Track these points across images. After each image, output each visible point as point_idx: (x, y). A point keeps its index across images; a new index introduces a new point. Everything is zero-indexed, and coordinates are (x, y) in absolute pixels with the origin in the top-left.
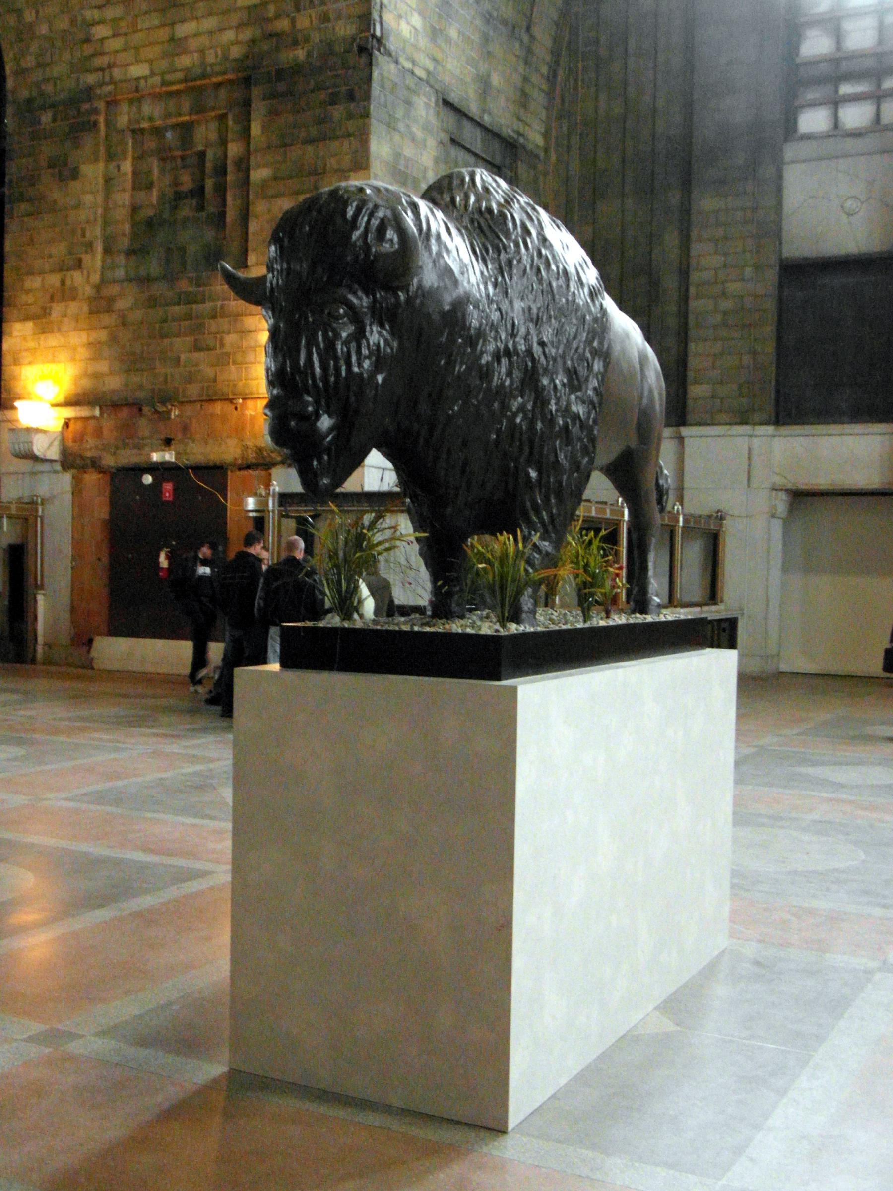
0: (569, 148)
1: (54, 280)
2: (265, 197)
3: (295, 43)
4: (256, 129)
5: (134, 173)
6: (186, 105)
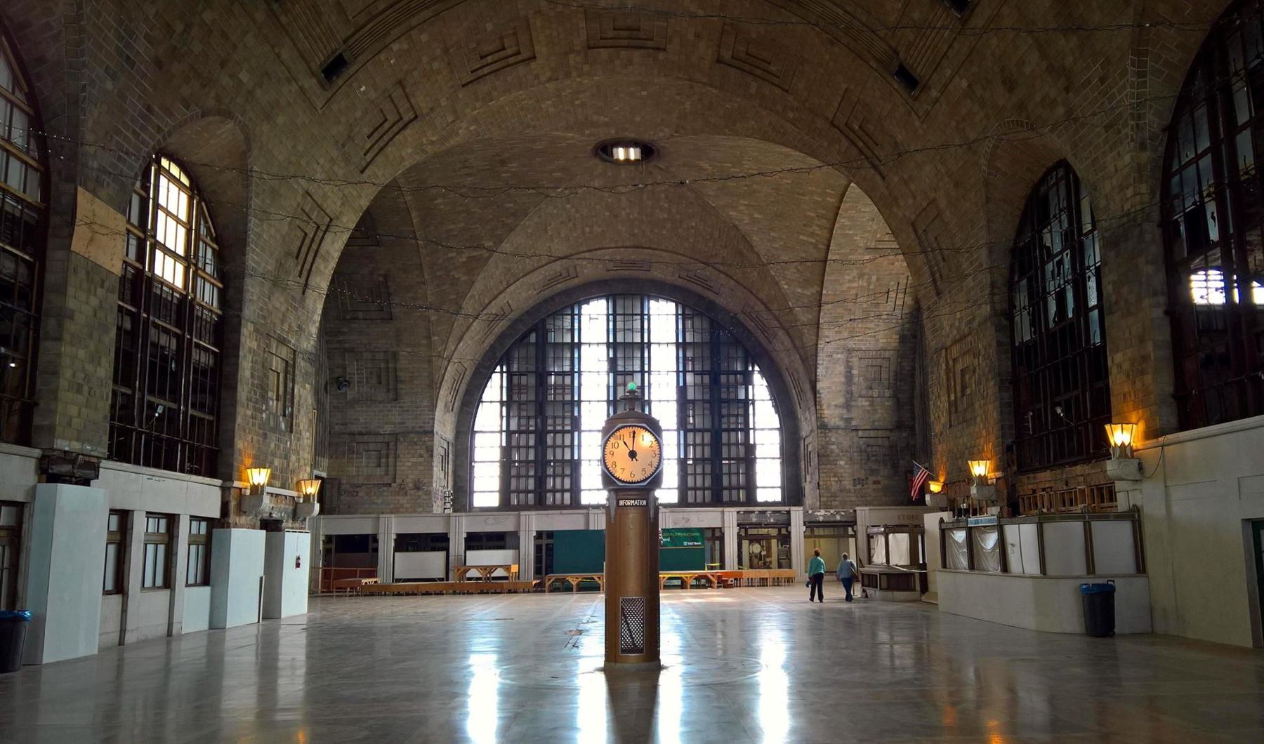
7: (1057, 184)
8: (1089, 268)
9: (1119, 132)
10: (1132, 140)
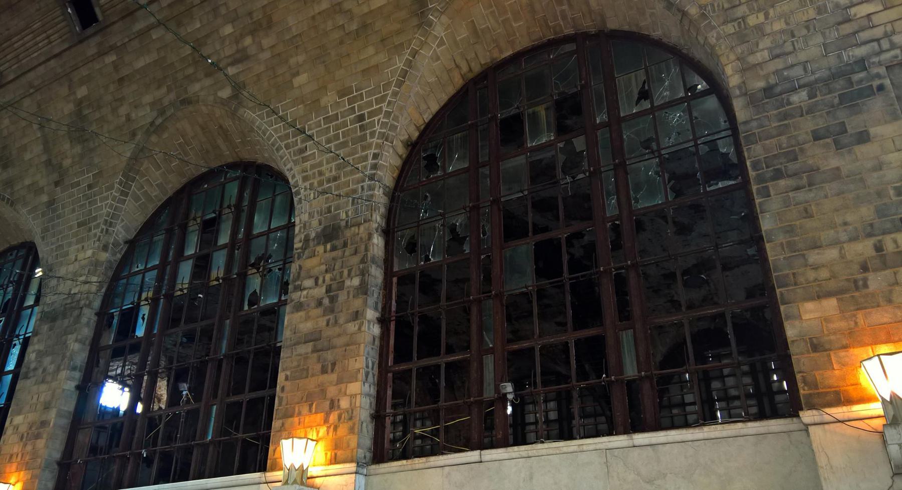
1: (864, 248)
7: (14, 261)
8: (18, 336)
9: (90, 230)
10: (99, 240)
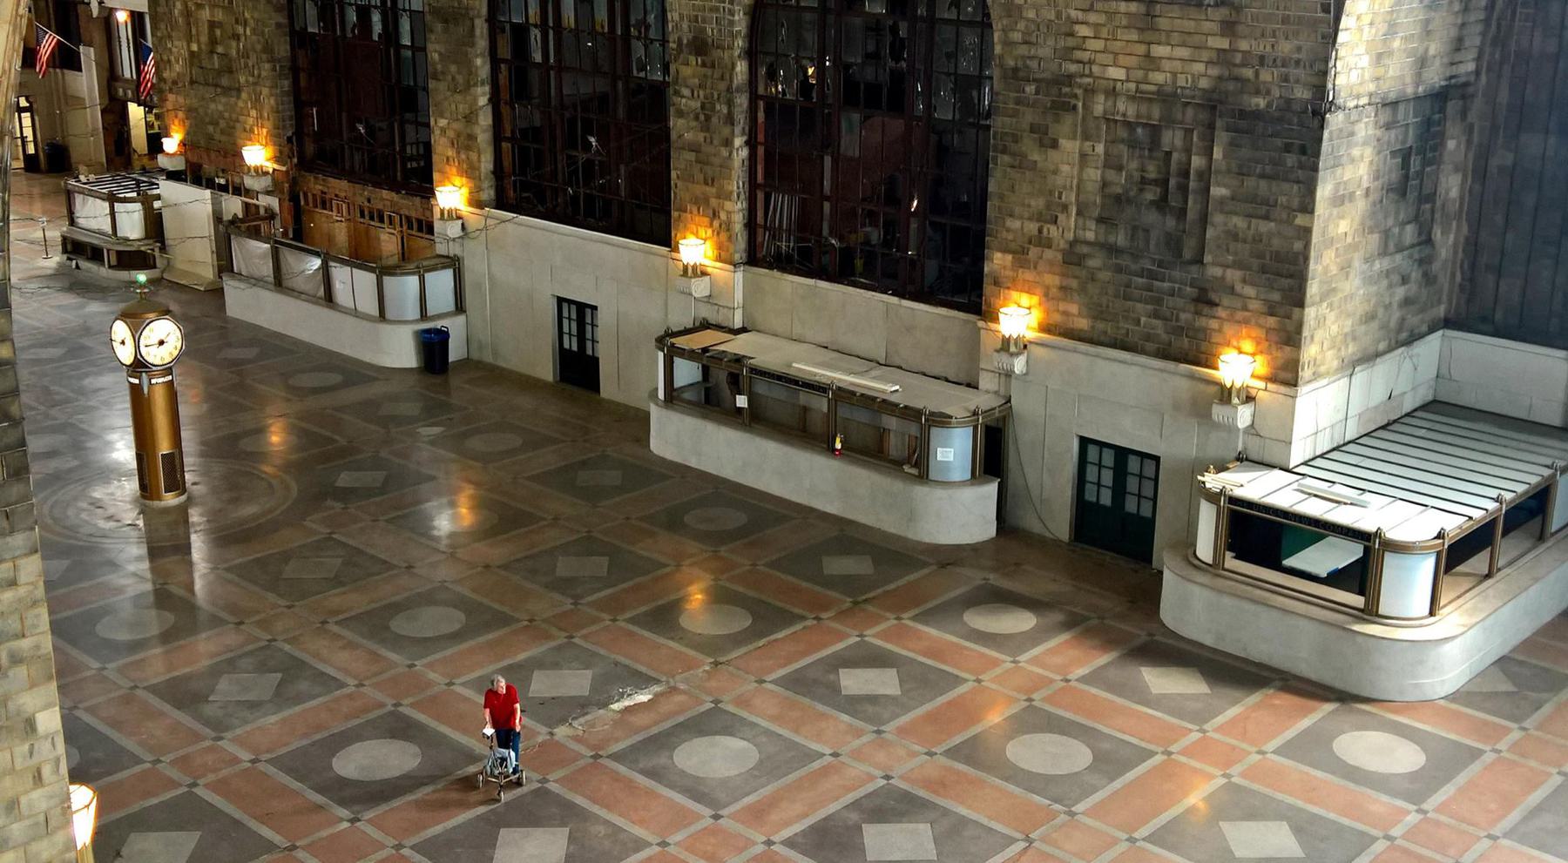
0: (1499, 76)
1: (1032, 227)
2: (1222, 212)
3: (1257, 93)
4: (1218, 153)
5: (1106, 153)
6: (1156, 112)
